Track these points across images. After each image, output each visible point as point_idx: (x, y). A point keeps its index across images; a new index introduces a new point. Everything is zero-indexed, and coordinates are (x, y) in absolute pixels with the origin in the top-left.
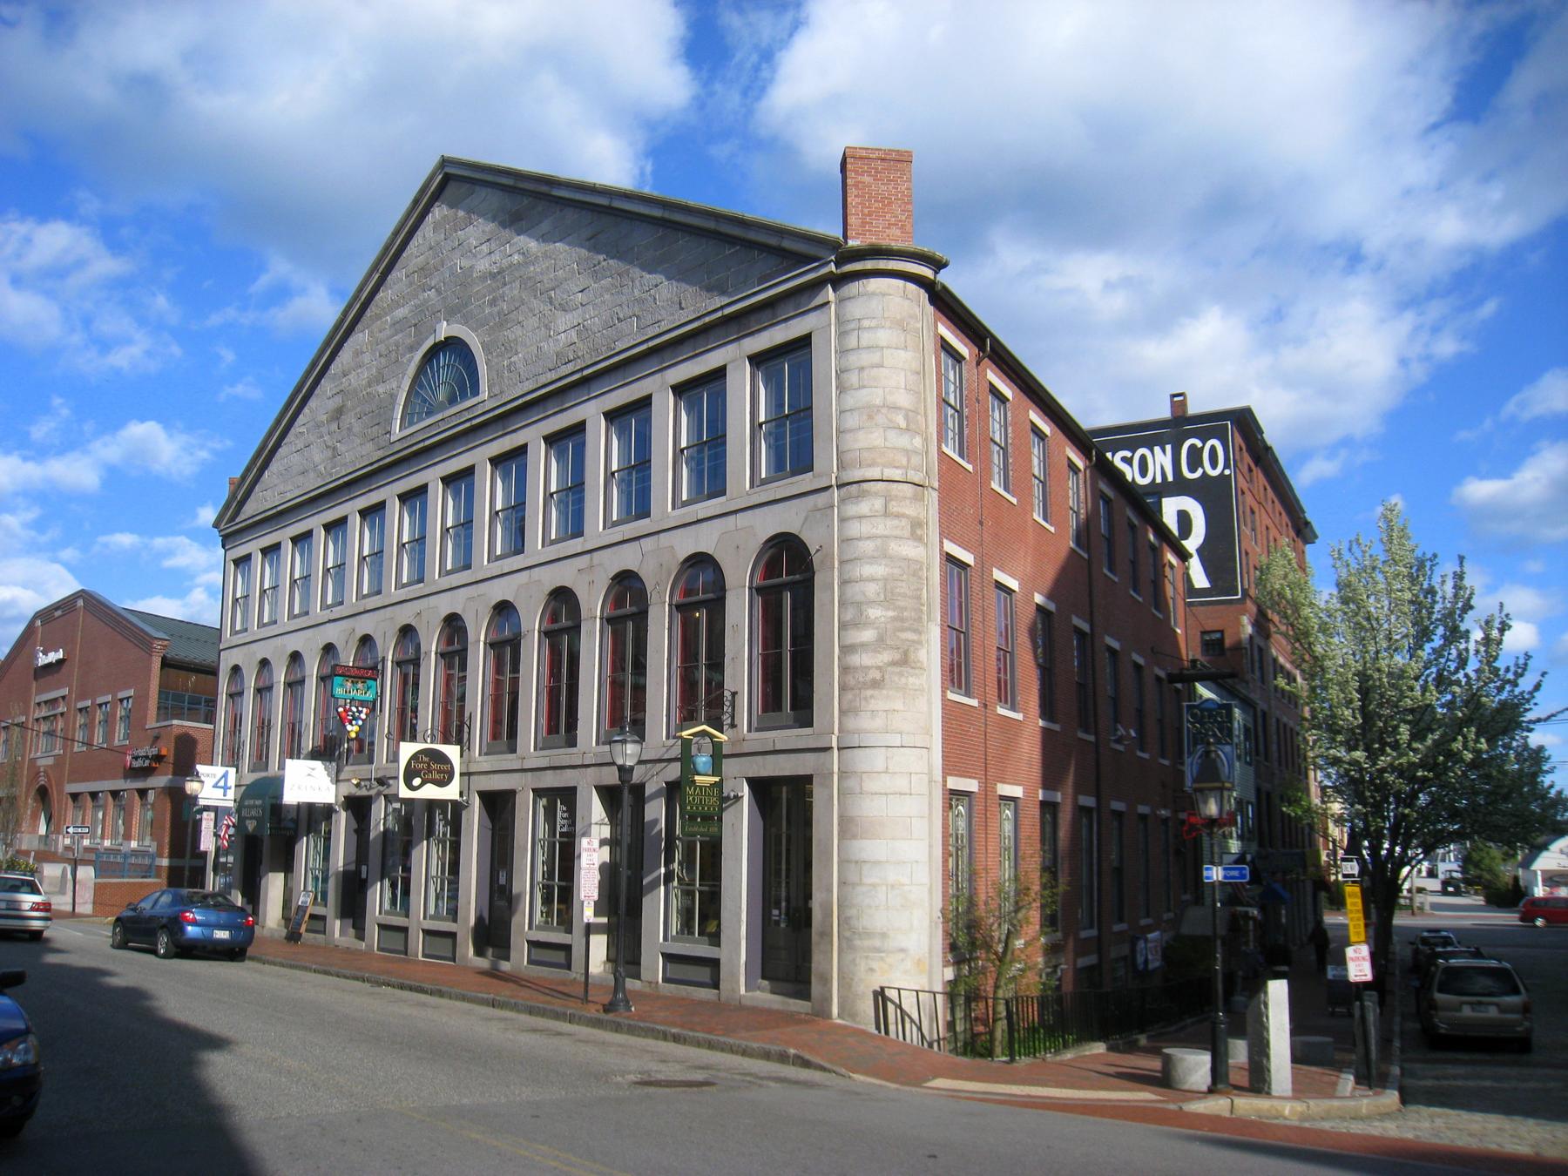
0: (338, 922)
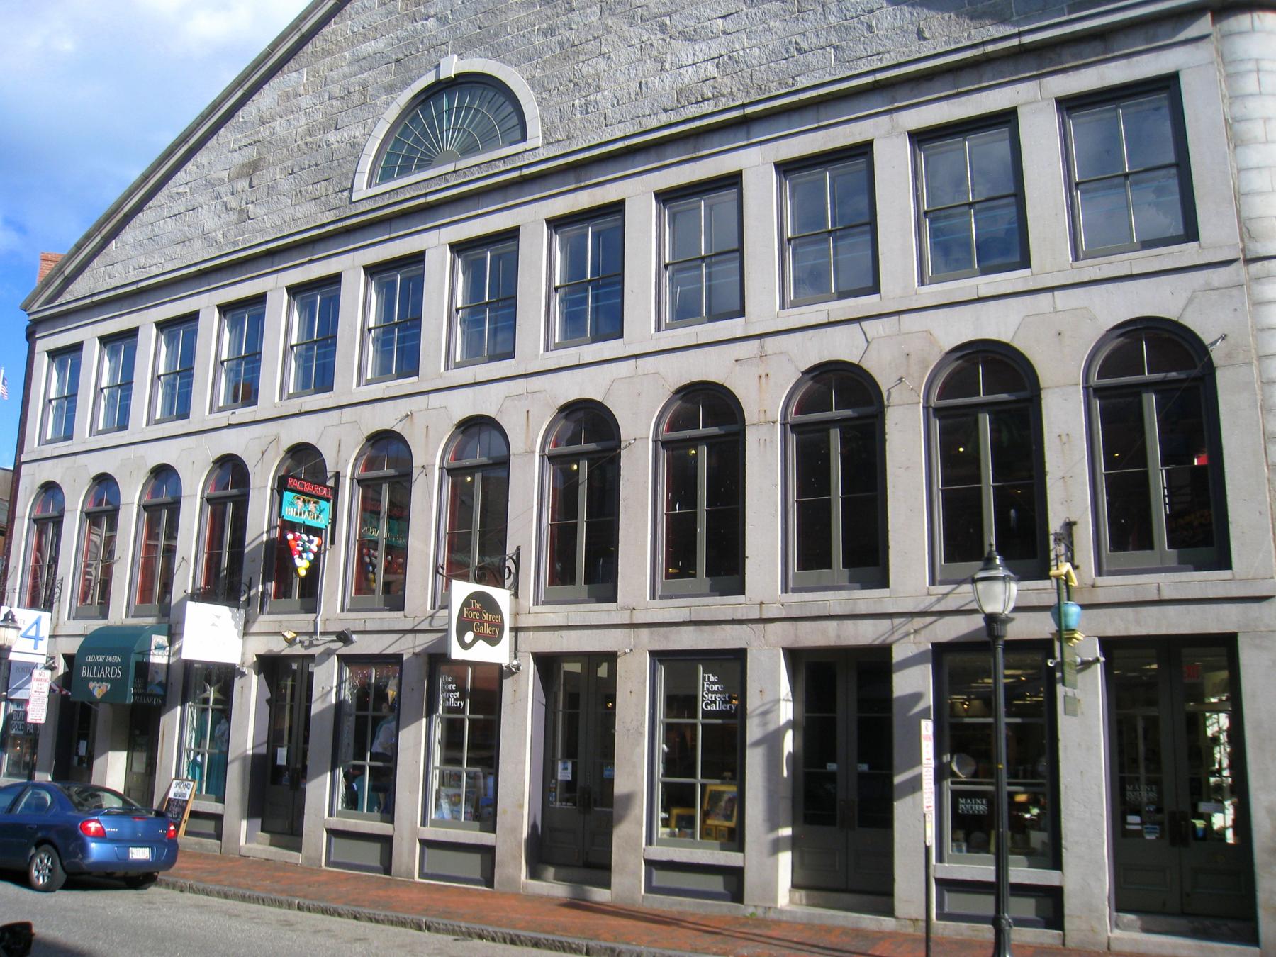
0: (244, 823)
